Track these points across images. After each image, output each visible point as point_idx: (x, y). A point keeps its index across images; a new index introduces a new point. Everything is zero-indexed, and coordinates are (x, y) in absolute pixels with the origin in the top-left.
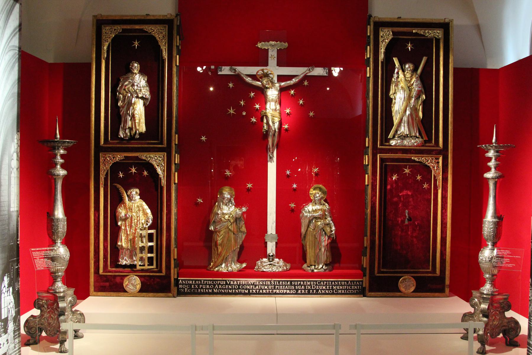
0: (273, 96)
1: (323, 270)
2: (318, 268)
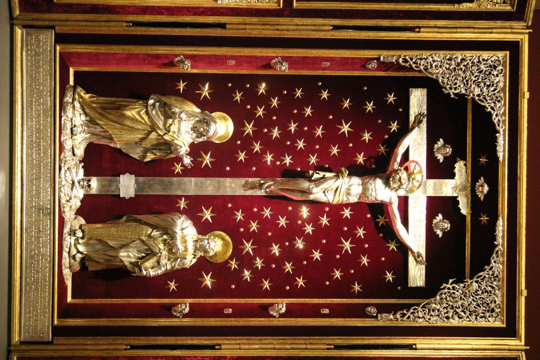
0: (374, 189)
2: (79, 243)
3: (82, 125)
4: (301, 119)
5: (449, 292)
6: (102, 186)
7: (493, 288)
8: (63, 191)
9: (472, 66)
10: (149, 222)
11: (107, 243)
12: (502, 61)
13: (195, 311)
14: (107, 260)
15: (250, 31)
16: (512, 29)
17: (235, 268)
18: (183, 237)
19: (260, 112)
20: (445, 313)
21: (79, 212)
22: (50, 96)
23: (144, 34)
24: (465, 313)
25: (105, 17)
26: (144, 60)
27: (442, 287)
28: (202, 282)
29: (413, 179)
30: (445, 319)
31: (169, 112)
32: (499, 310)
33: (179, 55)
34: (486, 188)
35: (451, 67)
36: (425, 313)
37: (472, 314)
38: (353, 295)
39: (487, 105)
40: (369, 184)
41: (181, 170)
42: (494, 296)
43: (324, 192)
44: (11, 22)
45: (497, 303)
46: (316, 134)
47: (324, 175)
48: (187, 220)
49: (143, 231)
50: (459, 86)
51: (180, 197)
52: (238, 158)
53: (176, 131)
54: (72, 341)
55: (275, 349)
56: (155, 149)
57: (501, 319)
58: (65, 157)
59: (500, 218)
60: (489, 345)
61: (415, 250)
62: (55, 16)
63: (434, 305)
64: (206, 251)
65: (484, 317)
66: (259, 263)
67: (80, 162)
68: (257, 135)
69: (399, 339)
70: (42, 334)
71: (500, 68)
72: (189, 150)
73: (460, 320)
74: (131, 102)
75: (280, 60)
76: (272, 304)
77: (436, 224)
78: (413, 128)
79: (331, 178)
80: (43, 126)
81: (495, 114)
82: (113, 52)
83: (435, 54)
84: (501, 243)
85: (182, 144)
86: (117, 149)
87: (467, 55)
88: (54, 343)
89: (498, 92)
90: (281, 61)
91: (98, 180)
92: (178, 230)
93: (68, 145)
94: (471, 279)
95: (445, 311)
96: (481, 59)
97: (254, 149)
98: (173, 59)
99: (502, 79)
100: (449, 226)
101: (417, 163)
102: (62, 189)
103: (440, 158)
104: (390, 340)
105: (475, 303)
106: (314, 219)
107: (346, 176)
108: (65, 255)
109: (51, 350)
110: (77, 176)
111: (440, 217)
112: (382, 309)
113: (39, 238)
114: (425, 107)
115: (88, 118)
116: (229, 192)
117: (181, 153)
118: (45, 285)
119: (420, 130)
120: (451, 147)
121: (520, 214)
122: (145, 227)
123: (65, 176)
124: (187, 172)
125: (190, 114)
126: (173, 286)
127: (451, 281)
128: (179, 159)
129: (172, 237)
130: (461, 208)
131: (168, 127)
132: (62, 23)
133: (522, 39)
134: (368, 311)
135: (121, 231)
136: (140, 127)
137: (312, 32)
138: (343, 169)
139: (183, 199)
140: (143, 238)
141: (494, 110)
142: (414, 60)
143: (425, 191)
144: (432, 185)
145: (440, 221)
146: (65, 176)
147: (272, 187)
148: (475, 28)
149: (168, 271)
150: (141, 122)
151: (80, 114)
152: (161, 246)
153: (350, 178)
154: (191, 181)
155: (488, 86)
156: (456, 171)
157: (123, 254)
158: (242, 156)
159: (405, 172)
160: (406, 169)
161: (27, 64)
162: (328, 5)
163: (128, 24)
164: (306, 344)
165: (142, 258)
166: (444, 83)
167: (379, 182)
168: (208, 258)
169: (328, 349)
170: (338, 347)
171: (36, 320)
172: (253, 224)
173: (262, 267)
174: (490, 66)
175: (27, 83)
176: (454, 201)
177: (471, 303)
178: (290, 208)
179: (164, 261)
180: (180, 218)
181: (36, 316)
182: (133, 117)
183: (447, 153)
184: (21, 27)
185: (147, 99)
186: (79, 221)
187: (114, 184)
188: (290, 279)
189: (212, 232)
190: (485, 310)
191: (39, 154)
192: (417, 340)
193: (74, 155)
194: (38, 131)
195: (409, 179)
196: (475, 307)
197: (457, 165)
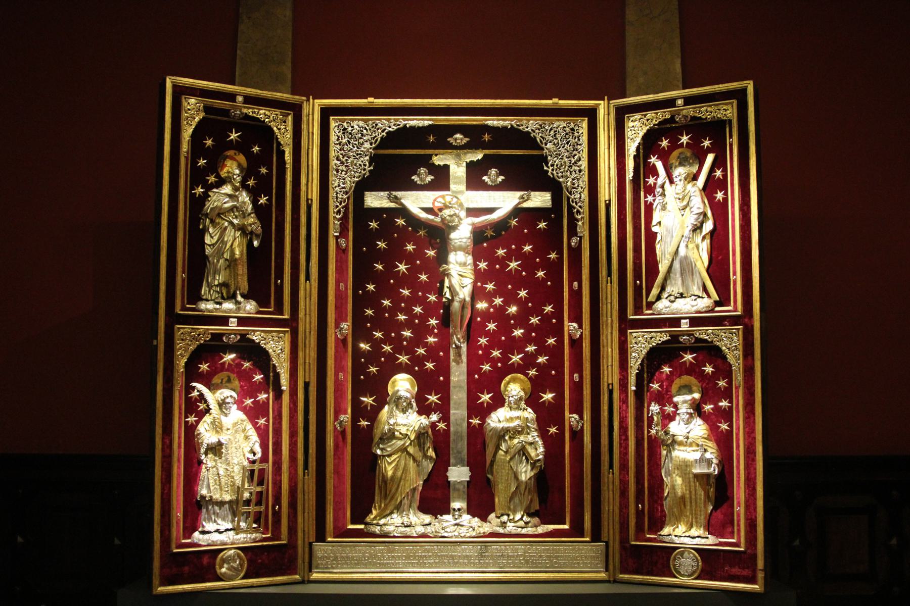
0: (460, 240)
1: (523, 523)
2: (514, 518)
3: (402, 517)
4: (394, 310)
5: (556, 170)
6: (459, 498)
7: (551, 129)
8: (465, 534)
9: (344, 151)
10: (493, 453)
11: (513, 493)
12: (339, 123)
13: (577, 408)
14: (529, 492)
15: (311, 359)
16: (309, 114)
17: (536, 371)
18: (507, 420)
19: (387, 348)
20: (576, 174)
21: (484, 518)
22: (374, 547)
23: (315, 459)
24: (576, 155)
25: (300, 496)
26: (339, 458)
27: (552, 176)
28: (549, 402)
29: (450, 204)
30: (581, 174)
31: (389, 435)
32: (572, 123)
33: (335, 426)
34: (458, 136)
35: (345, 170)
36: (576, 192)
37: (576, 149)
38: (560, 259)
39: (380, 136)
40: (455, 245)
41: (443, 423)
42: (559, 128)
43: (463, 287)
44: (306, 583)
45: (565, 125)
46: (408, 296)
47: (447, 287)
48: (491, 417)
49: (501, 459)
50: (362, 162)
51: (469, 424)
52: (431, 369)
53: (406, 428)
54: (606, 523)
55: (612, 333)
56: (424, 448)
57: (580, 122)
58: (433, 532)
59: (486, 123)
60: (604, 133)
61: (517, 201)
62: (300, 542)
63: (569, 184)
64: (520, 399)
65: (578, 138)
66: (531, 348)
67: (436, 518)
68: (410, 351)
69: (600, 216)
70: (598, 551)
71: (345, 124)
72: (424, 416)
73: (582, 159)
74: (379, 471)
75: (338, 330)
76: (570, 335)
77: (492, 182)
78: (402, 204)
79: (450, 281)
80: (403, 553)
81: (388, 128)
82: (332, 488)
83: (333, 184)
84: (510, 122)
85: (419, 422)
86: (424, 484)
87: (333, 155)
88: (606, 540)
89: (368, 126)
90: (339, 329)
91: (454, 502)
92: (500, 426)
93: (420, 530)
94: (543, 150)
95: (574, 173)
96: (337, 142)
97: (423, 354)
98: (338, 431)
99: (356, 122)
100: (494, 170)
101: (435, 200)
102: (462, 535)
103: (429, 178)
104: (602, 224)
105: (566, 146)
106: (489, 297)
107: (447, 266)
108: (524, 531)
109: (614, 543)
110: (449, 521)
111: (485, 178)
112: (573, 232)
113: (508, 556)
114: (382, 193)
115: (395, 511)
116: (464, 377)
117: (427, 423)
118: (553, 550)
119: (404, 198)
120: (420, 168)
121: (482, 105)
122: (498, 457)
123: (450, 532)
124: (446, 418)
125: (390, 415)
126: (553, 430)
127: (545, 168)
128: (433, 425)
129: (507, 431)
130: (477, 159)
131: (402, 435)
132: (306, 536)
133: (319, 105)
134: (575, 245)
135: (501, 479)
136: (403, 462)
137: (312, 301)
138: (441, 269)
139: (471, 421)
140: (508, 458)
141: (385, 129)
142: (338, 204)
143: (461, 192)
144: (455, 186)
145: (489, 178)
146: (450, 532)
147: (459, 336)
148: (308, 148)
149: (539, 435)
150: (398, 462)
151: (391, 518)
152: (516, 441)
153: (450, 263)
154: (454, 413)
155: (362, 135)
156: (442, 163)
157: (523, 478)
158: (430, 365)
159: (444, 211)
160: (441, 210)
161: (345, 568)
162: (287, 285)
163: (306, 474)
164: (607, 303)
165: (527, 459)
166: (360, 176)
167: (453, 235)
168: (527, 397)
169: (611, 283)
170: (609, 274)
171: (586, 557)
172: (494, 354)
173: (535, 346)
174: (344, 133)
175: (363, 568)
176: (470, 166)
177: (565, 149)
178: (479, 319)
179: (530, 439)
180: (489, 424)
181: (582, 558)
182: (393, 469)
183: (425, 172)
184: (310, 573)
185: (376, 456)
186: (492, 519)
187: (457, 486)
188: (546, 318)
189: (502, 393)
190: (573, 136)
191: (430, 556)
192: (601, 199)
193: (430, 524)
194: (408, 557)
195: (450, 207)
196: (570, 146)
197: (437, 163)
